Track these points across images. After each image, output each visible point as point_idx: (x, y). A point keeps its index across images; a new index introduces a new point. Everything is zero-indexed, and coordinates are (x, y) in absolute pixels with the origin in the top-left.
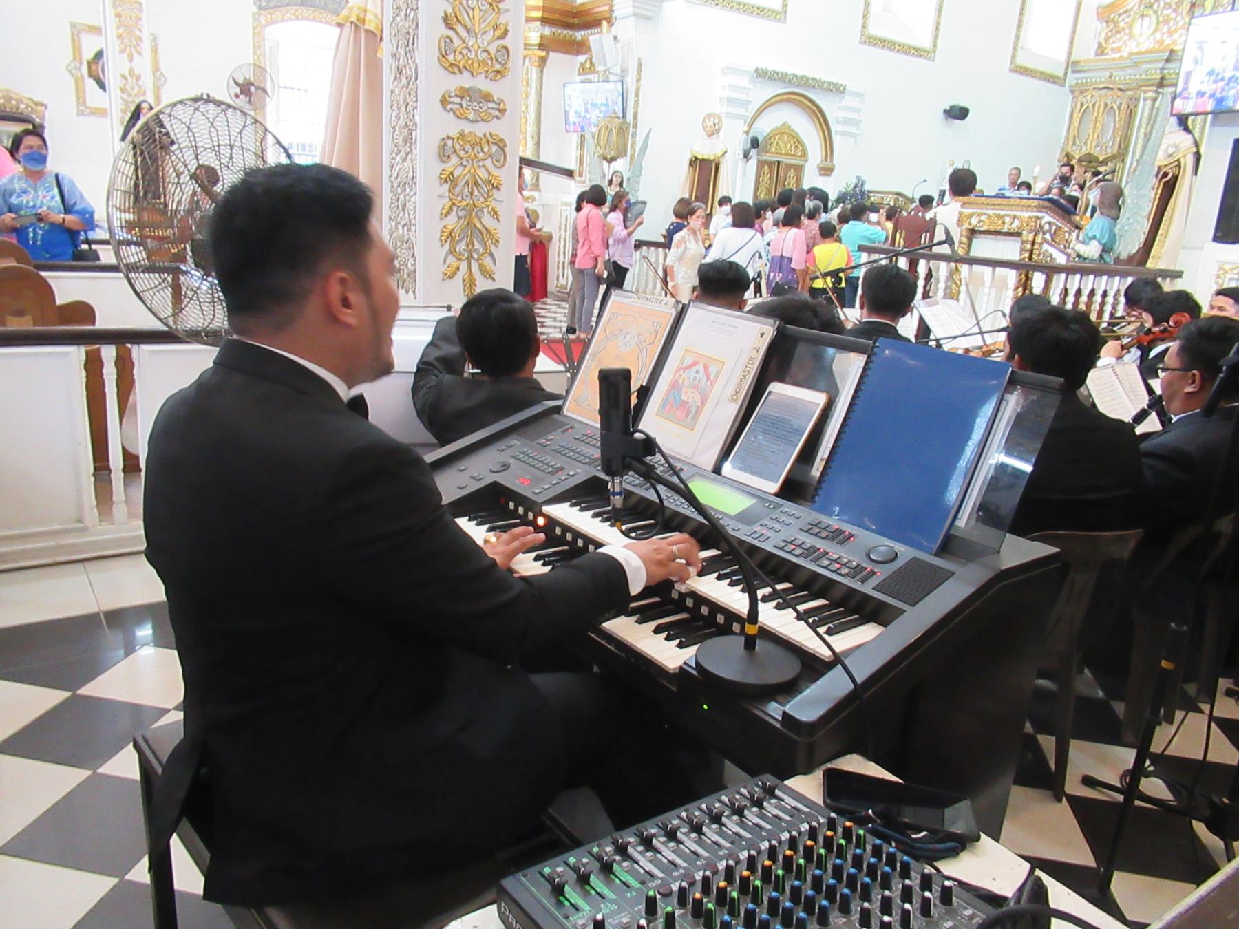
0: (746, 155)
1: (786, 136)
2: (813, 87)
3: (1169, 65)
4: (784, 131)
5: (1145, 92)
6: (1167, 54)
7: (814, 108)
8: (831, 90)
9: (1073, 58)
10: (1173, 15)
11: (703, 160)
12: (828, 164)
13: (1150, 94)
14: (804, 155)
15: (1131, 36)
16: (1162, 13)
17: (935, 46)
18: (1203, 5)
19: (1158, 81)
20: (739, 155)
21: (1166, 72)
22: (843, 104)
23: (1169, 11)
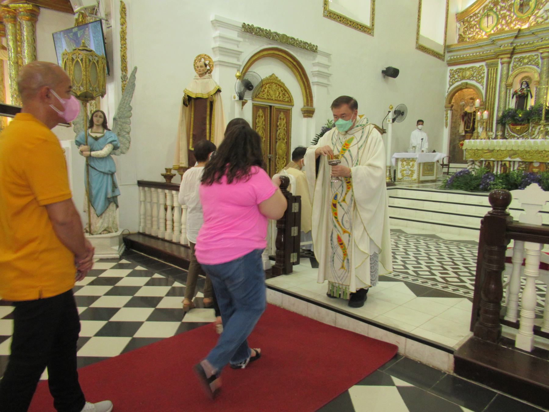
0: (241, 97)
1: (274, 86)
2: (293, 45)
3: (517, 40)
4: (273, 81)
5: (501, 59)
6: (517, 32)
7: (295, 63)
8: (307, 49)
9: (447, 44)
10: (508, 13)
11: (197, 99)
13: (506, 60)
14: (290, 101)
15: (480, 29)
17: (373, 25)
18: (528, 5)
19: (512, 50)
20: (234, 98)
21: (514, 45)
22: (316, 61)
23: (505, 11)
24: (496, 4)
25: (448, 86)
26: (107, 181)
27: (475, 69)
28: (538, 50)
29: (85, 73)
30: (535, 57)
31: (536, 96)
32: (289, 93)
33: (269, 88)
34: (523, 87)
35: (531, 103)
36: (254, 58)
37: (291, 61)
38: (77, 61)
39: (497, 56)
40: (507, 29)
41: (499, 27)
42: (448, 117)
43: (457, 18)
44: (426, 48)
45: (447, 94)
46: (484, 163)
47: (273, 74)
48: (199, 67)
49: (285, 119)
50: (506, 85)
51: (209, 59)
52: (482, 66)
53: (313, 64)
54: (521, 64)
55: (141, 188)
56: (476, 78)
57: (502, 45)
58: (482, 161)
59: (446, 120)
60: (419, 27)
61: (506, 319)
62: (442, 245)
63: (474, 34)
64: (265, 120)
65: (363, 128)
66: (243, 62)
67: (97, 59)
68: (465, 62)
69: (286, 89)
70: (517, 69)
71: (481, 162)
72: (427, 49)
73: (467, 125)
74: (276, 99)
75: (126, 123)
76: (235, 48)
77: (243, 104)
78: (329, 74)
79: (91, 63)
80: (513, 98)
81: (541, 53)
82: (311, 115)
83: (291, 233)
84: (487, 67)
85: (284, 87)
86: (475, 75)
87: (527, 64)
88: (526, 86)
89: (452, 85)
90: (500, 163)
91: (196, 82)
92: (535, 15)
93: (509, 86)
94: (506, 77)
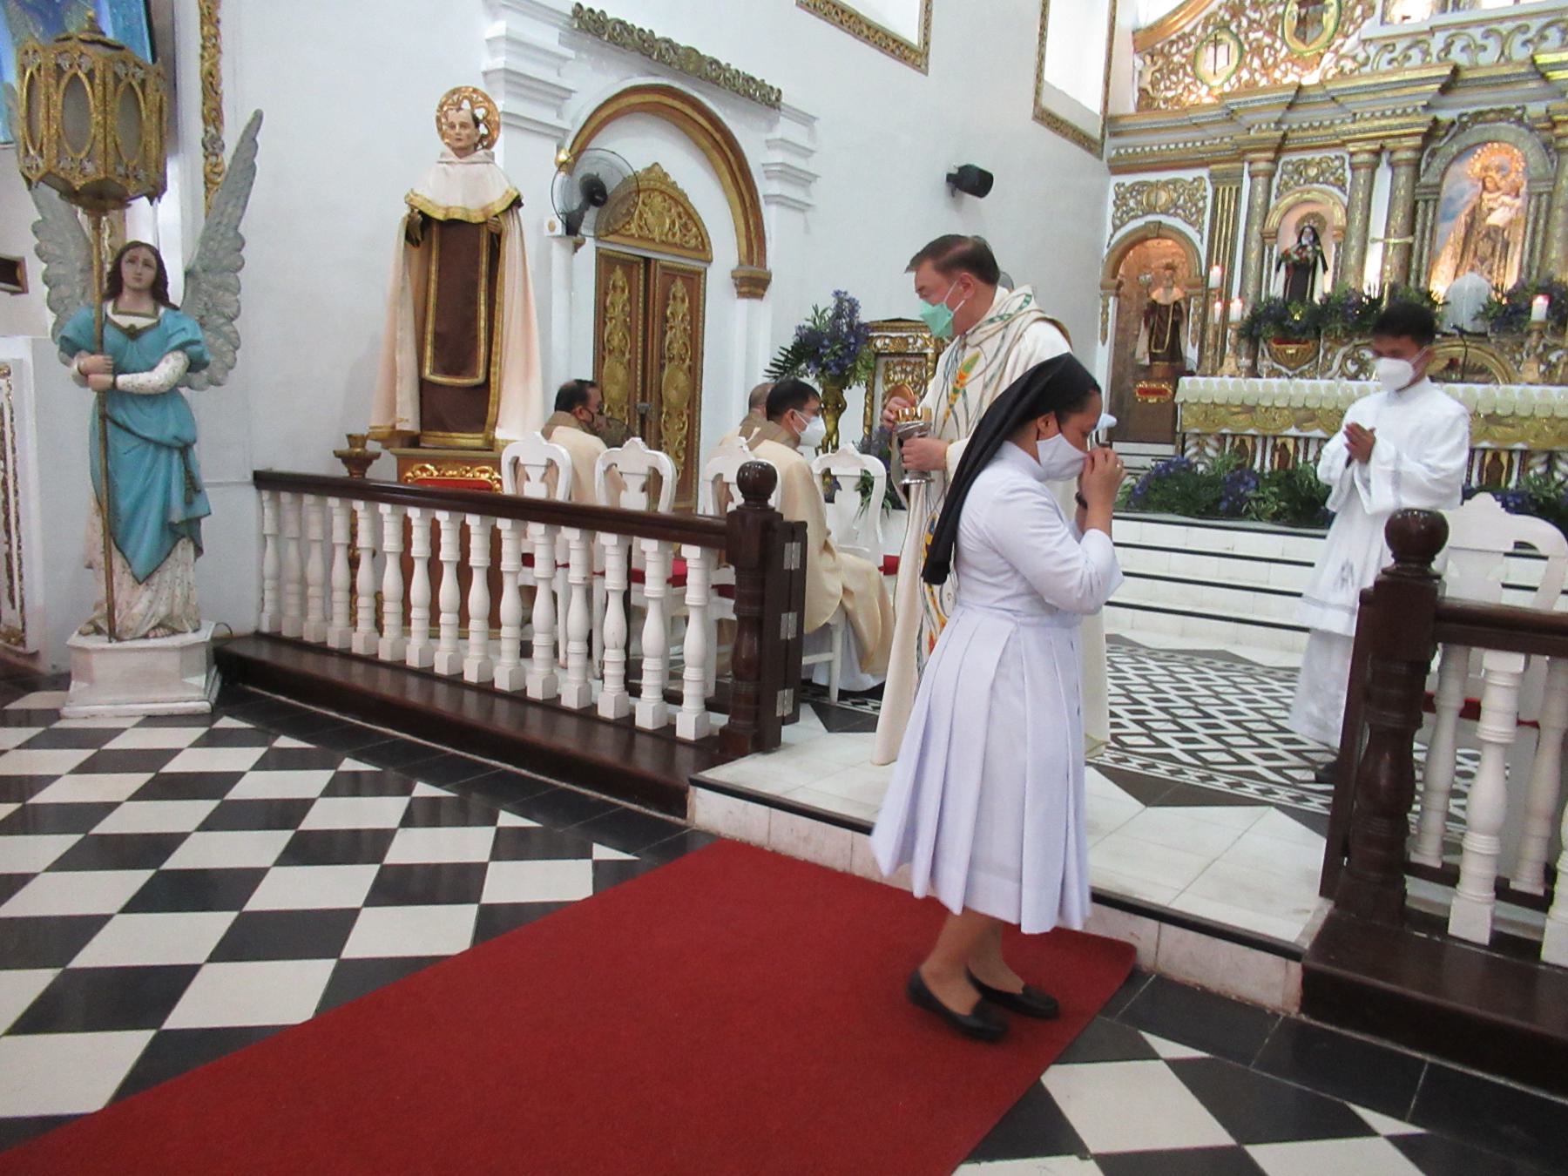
0: (572, 227)
2: (715, 81)
3: (1291, 116)
5: (1251, 163)
6: (1293, 92)
7: (718, 136)
10: (1267, 40)
12: (754, 270)
13: (1262, 166)
14: (703, 248)
15: (1196, 77)
16: (1247, 37)
17: (926, 44)
18: (1320, 21)
19: (1279, 141)
20: (552, 227)
21: (1285, 127)
23: (1260, 34)
24: (1237, 11)
25: (1110, 229)
26: (169, 472)
27: (1182, 186)
28: (1344, 144)
29: (100, 118)
30: (1337, 163)
31: (1335, 267)
32: (700, 225)
33: (644, 203)
34: (1304, 241)
35: (1324, 284)
36: (603, 114)
37: (707, 130)
38: (76, 76)
39: (1240, 154)
40: (1263, 82)
41: (1245, 75)
42: (1107, 314)
43: (1135, 41)
44: (1057, 120)
45: (1106, 251)
46: (1229, 440)
47: (657, 164)
48: (457, 127)
49: (687, 301)
50: (1261, 234)
51: (486, 104)
52: (1201, 178)
53: (767, 141)
54: (1299, 179)
55: (266, 495)
56: (1184, 211)
57: (1253, 126)
58: (1225, 436)
59: (1105, 323)
60: (1042, 57)
61: (1415, 858)
62: (1151, 664)
63: (1180, 91)
64: (630, 299)
65: (1007, 326)
66: (574, 121)
67: (140, 74)
68: (1158, 165)
69: (691, 211)
70: (1291, 192)
71: (1222, 438)
72: (1063, 122)
73: (1157, 337)
74: (664, 238)
75: (225, 288)
76: (553, 78)
77: (577, 246)
78: (811, 174)
79: (122, 87)
80: (1278, 269)
81: (1352, 154)
82: (760, 291)
83: (779, 633)
84: (1212, 183)
85: (686, 205)
86: (1181, 201)
87: (1316, 180)
88: (1311, 238)
89: (1119, 227)
90: (1270, 443)
91: (446, 173)
92: (1336, 51)
93: (1268, 238)
94: (1263, 213)
